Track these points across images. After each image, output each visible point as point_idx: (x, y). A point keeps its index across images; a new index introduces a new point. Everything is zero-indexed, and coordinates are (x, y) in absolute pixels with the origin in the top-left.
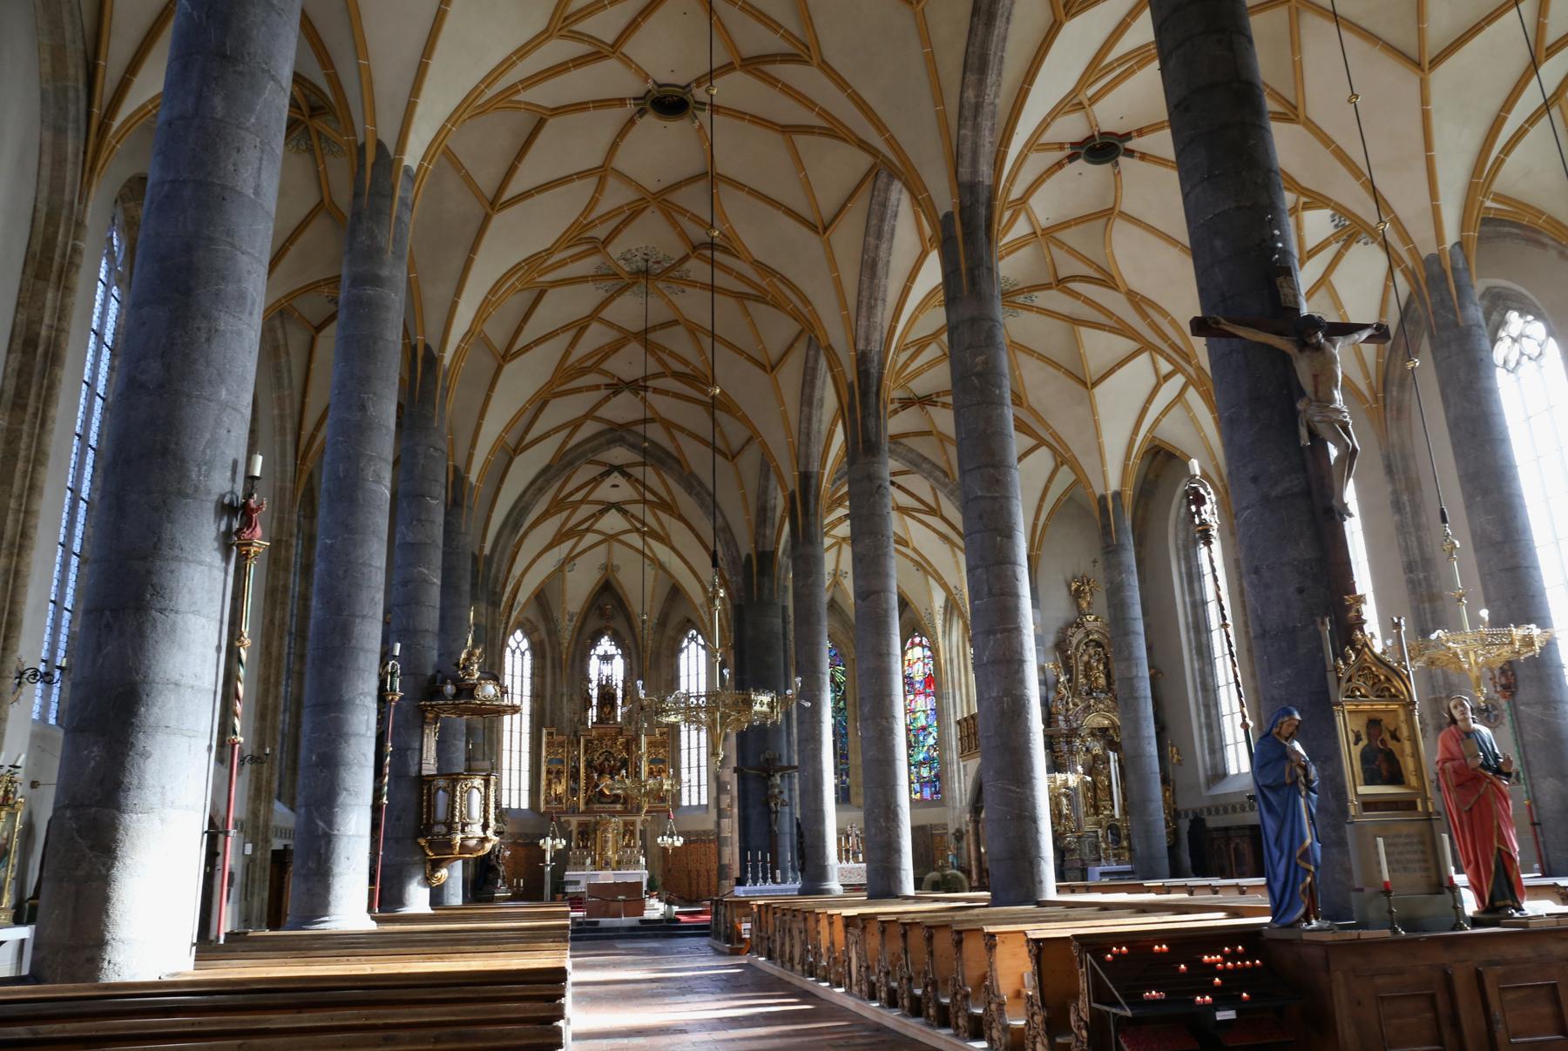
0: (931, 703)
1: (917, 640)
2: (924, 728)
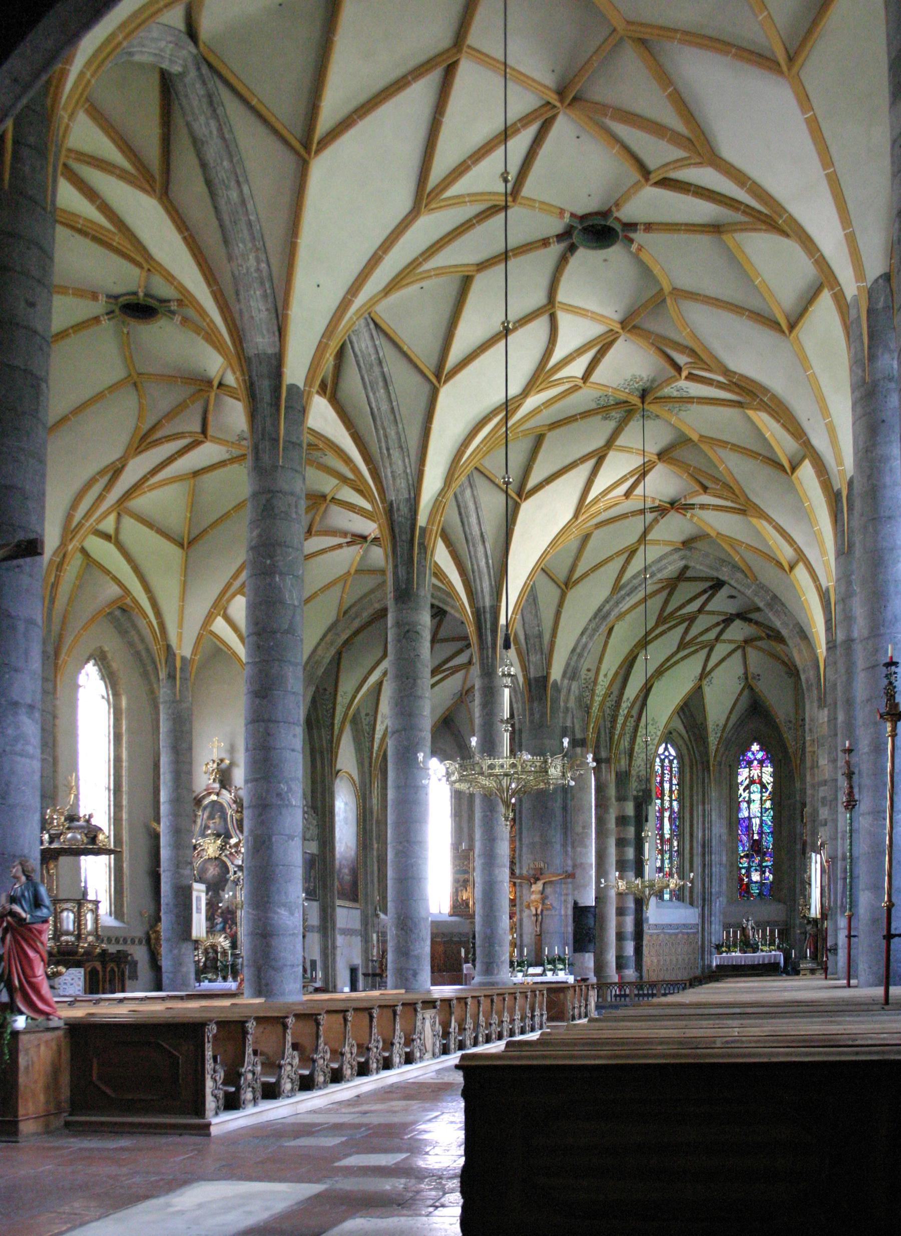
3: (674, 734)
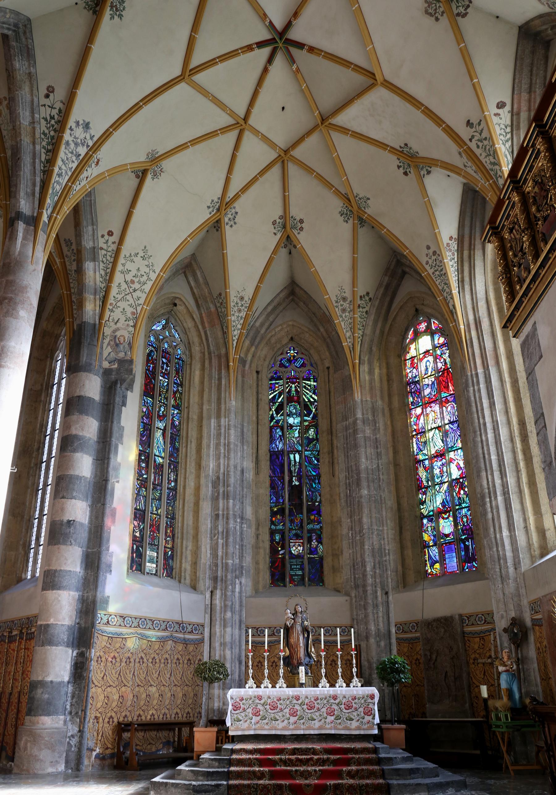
0: (450, 412)
1: (423, 326)
2: (440, 455)
3: (180, 308)
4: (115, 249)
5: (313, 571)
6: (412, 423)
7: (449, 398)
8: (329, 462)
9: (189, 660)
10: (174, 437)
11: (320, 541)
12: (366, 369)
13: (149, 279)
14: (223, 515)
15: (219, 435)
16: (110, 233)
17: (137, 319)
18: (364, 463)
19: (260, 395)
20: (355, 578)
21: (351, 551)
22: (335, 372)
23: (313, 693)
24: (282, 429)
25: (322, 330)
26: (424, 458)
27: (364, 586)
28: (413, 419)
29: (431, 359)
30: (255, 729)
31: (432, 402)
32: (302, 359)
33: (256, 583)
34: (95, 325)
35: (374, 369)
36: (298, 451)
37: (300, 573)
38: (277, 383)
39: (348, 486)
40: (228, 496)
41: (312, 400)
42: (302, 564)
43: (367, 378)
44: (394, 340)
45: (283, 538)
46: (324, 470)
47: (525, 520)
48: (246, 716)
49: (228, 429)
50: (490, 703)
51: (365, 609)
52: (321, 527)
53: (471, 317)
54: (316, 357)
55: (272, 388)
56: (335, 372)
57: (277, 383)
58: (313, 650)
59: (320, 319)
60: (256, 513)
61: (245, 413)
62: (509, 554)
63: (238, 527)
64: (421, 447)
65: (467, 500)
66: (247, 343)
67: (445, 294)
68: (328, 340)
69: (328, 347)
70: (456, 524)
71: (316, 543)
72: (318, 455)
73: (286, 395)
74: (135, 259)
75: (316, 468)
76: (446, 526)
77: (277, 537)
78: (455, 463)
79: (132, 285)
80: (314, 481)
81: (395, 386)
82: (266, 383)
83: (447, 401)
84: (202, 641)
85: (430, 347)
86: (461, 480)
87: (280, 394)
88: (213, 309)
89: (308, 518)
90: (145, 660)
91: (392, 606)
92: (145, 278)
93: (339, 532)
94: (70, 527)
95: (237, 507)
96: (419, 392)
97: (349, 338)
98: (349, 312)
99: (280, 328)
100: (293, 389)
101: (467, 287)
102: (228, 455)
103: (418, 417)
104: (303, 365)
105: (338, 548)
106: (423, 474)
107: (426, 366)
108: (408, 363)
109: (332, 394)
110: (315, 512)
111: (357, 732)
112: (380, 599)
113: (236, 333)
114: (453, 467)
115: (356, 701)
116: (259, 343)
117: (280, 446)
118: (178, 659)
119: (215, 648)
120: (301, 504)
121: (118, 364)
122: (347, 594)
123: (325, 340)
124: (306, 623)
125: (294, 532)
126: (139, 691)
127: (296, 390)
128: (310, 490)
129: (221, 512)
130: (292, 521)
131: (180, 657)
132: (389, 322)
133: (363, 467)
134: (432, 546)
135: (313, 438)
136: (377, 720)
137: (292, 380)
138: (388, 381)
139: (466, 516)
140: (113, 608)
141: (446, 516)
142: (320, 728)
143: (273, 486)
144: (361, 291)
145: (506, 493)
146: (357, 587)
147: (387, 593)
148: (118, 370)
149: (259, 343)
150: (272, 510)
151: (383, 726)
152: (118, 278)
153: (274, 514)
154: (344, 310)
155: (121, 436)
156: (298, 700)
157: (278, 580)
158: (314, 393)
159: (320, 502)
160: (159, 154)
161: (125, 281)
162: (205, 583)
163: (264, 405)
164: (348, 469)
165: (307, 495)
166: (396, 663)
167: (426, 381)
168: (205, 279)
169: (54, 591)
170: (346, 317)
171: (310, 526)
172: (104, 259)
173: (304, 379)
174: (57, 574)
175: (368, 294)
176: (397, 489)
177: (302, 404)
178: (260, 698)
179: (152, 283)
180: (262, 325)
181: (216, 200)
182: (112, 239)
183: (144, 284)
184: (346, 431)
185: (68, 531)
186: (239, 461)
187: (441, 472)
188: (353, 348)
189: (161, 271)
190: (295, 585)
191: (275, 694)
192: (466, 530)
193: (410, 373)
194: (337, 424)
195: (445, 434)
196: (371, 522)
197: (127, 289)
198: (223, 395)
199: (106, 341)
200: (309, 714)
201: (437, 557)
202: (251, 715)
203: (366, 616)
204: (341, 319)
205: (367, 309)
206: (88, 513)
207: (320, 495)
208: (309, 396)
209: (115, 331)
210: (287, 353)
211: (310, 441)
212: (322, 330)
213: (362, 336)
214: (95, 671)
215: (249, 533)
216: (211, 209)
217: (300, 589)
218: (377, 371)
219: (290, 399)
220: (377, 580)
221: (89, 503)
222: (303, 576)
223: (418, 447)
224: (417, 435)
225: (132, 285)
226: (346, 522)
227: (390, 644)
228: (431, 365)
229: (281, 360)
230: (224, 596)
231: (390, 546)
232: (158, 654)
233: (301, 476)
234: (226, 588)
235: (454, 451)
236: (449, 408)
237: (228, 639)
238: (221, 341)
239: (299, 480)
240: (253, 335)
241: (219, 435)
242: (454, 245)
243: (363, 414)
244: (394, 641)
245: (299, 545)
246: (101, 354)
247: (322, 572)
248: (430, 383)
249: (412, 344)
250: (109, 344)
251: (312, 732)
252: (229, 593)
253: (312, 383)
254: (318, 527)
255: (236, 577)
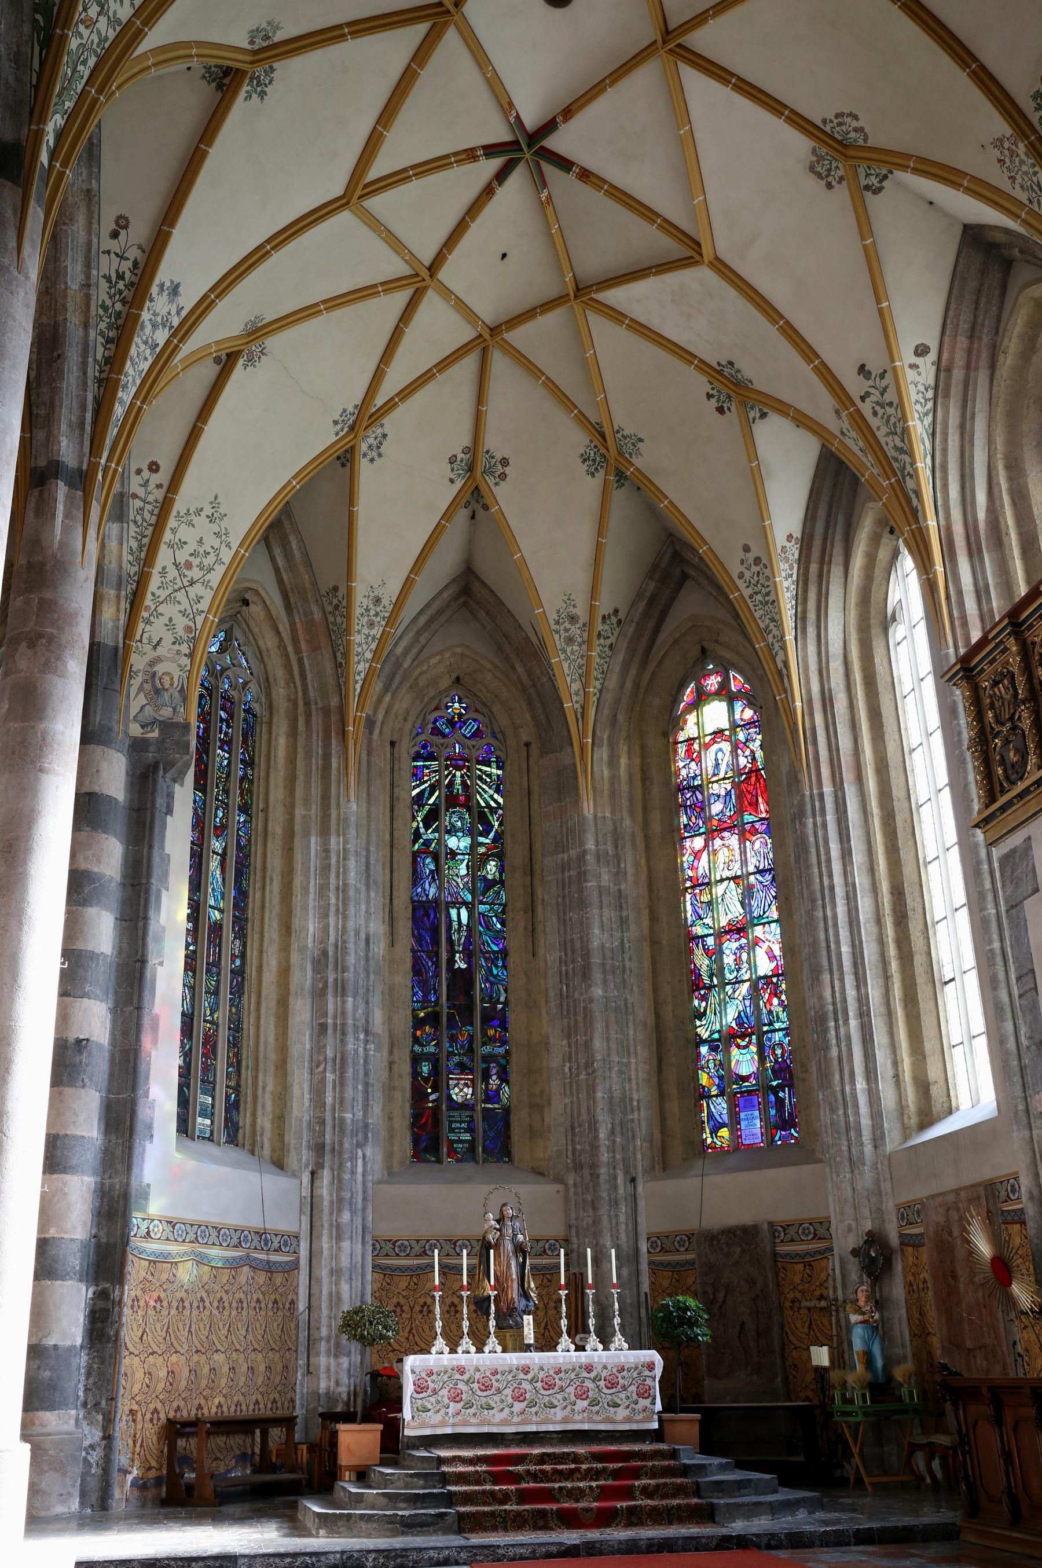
0: (759, 851)
1: (713, 682)
2: (738, 929)
3: (255, 609)
4: (160, 500)
5: (492, 1134)
6: (686, 865)
7: (757, 825)
8: (525, 928)
9: (276, 1302)
10: (242, 868)
11: (504, 1077)
12: (605, 756)
13: (219, 561)
14: (335, 1025)
15: (326, 868)
16: (154, 467)
17: (195, 641)
18: (598, 937)
19: (396, 790)
20: (574, 1150)
21: (567, 1101)
22: (541, 755)
23: (552, 1361)
24: (436, 857)
25: (520, 669)
26: (706, 932)
27: (594, 1166)
28: (688, 858)
29: (726, 746)
30: (453, 1425)
31: (724, 830)
32: (475, 720)
33: (389, 1156)
34: (116, 649)
35: (619, 757)
36: (465, 903)
37: (467, 1137)
38: (428, 767)
39: (565, 977)
40: (343, 988)
41: (493, 804)
42: (471, 1121)
43: (606, 773)
44: (656, 701)
45: (435, 1071)
46: (516, 942)
47: (896, 1064)
48: (438, 1402)
49: (345, 859)
50: (834, 1376)
51: (595, 1209)
52: (507, 1052)
53: (815, 688)
54: (503, 721)
55: (417, 775)
56: (541, 755)
57: (428, 767)
58: (532, 1285)
59: (519, 649)
60: (389, 1020)
61: (373, 825)
62: (865, 1121)
63: (361, 1050)
64: (701, 912)
65: (783, 1016)
66: (377, 686)
67: (770, 638)
68: (532, 692)
69: (530, 702)
70: (762, 1058)
71: (498, 1082)
72: (503, 912)
73: (444, 790)
74: (196, 520)
75: (498, 936)
76: (744, 1061)
77: (425, 1069)
78: (765, 946)
79: (187, 572)
80: (494, 962)
81: (656, 791)
82: (407, 765)
83: (754, 831)
84: (295, 1266)
85: (725, 725)
86: (775, 980)
87: (433, 789)
88: (317, 616)
89: (484, 1033)
90: (207, 1304)
91: (642, 1204)
92: (211, 559)
93: (545, 1063)
94: (80, 1052)
95: (360, 1011)
96: (700, 808)
97: (577, 694)
98: (580, 645)
99: (438, 657)
100: (458, 780)
101: (811, 631)
102: (345, 910)
103: (697, 855)
104: (477, 734)
105: (542, 1092)
106: (702, 962)
107: (716, 760)
108: (682, 749)
109: (535, 797)
110: (497, 1022)
111: (626, 1427)
112: (621, 1190)
113: (362, 667)
114: (760, 953)
115: (625, 1373)
116: (399, 686)
117: (432, 892)
118: (258, 1301)
119: (319, 1280)
120: (470, 1007)
121: (161, 731)
122: (559, 1180)
123: (524, 690)
124: (520, 1237)
125: (456, 1059)
126: (198, 1362)
127: (464, 783)
128: (487, 980)
129: (330, 1021)
130: (453, 1039)
131: (261, 1297)
132: (651, 667)
133: (596, 943)
134: (716, 1096)
135: (494, 880)
136: (658, 1407)
137: (456, 762)
138: (643, 780)
139: (781, 1044)
140: (156, 1206)
141: (743, 1044)
142: (565, 1420)
143: (417, 969)
144: (604, 606)
145: (864, 1014)
146: (578, 1167)
147: (633, 1180)
148: (161, 741)
149: (399, 686)
150: (415, 1017)
151: (665, 1415)
152: (164, 557)
153: (418, 1023)
154: (570, 640)
155: (166, 874)
156: (527, 1373)
157: (426, 1150)
158: (498, 791)
159: (506, 1004)
160: (264, 322)
161: (175, 564)
162: (301, 1156)
163: (403, 810)
164: (566, 945)
165: (481, 989)
166: (688, 1309)
167: (715, 789)
168: (305, 554)
169: (55, 1176)
170: (572, 653)
171: (487, 1049)
172: (138, 518)
173: (479, 763)
174: (59, 1143)
175: (616, 611)
176: (656, 988)
177: (475, 810)
178: (461, 1370)
179: (223, 568)
180: (407, 651)
181: (351, 409)
182: (155, 479)
183: (211, 569)
184: (563, 872)
185: (77, 1059)
186: (362, 922)
187: (738, 961)
188: (583, 714)
189: (241, 545)
190: (458, 1161)
191: (488, 1363)
192: (781, 1070)
193: (685, 769)
194: (543, 856)
195: (748, 893)
196: (609, 1048)
197: (178, 580)
198: (333, 790)
199: (136, 682)
200: (545, 1396)
201: (726, 1118)
202: (446, 1401)
203: (596, 1222)
204: (562, 657)
205: (612, 640)
206: (108, 1025)
207: (506, 991)
208: (487, 796)
209: (153, 663)
210: (447, 708)
211: (489, 884)
212: (520, 669)
213: (601, 691)
214: (131, 1326)
215: (379, 1058)
216: (339, 427)
217: (469, 1167)
218: (623, 761)
219: (452, 801)
220: (618, 1157)
221: (110, 1005)
222: (472, 1143)
223: (695, 912)
224: (693, 887)
225: (187, 572)
226: (558, 1045)
227: (638, 1273)
228: (726, 759)
229: (436, 720)
230: (338, 1182)
231: (641, 1093)
232: (227, 1292)
233: (471, 952)
234: (341, 1166)
235: (764, 924)
236: (757, 845)
237: (345, 1262)
238: (331, 681)
239: (468, 956)
240: (391, 669)
241: (326, 868)
242: (794, 551)
243: (597, 844)
244: (644, 1267)
245: (466, 1085)
246: (127, 707)
247: (508, 1137)
248: (723, 793)
249: (690, 712)
250: (141, 689)
251: (551, 1428)
252: (347, 1177)
253: (494, 771)
254: (502, 1050)
255: (358, 1145)
